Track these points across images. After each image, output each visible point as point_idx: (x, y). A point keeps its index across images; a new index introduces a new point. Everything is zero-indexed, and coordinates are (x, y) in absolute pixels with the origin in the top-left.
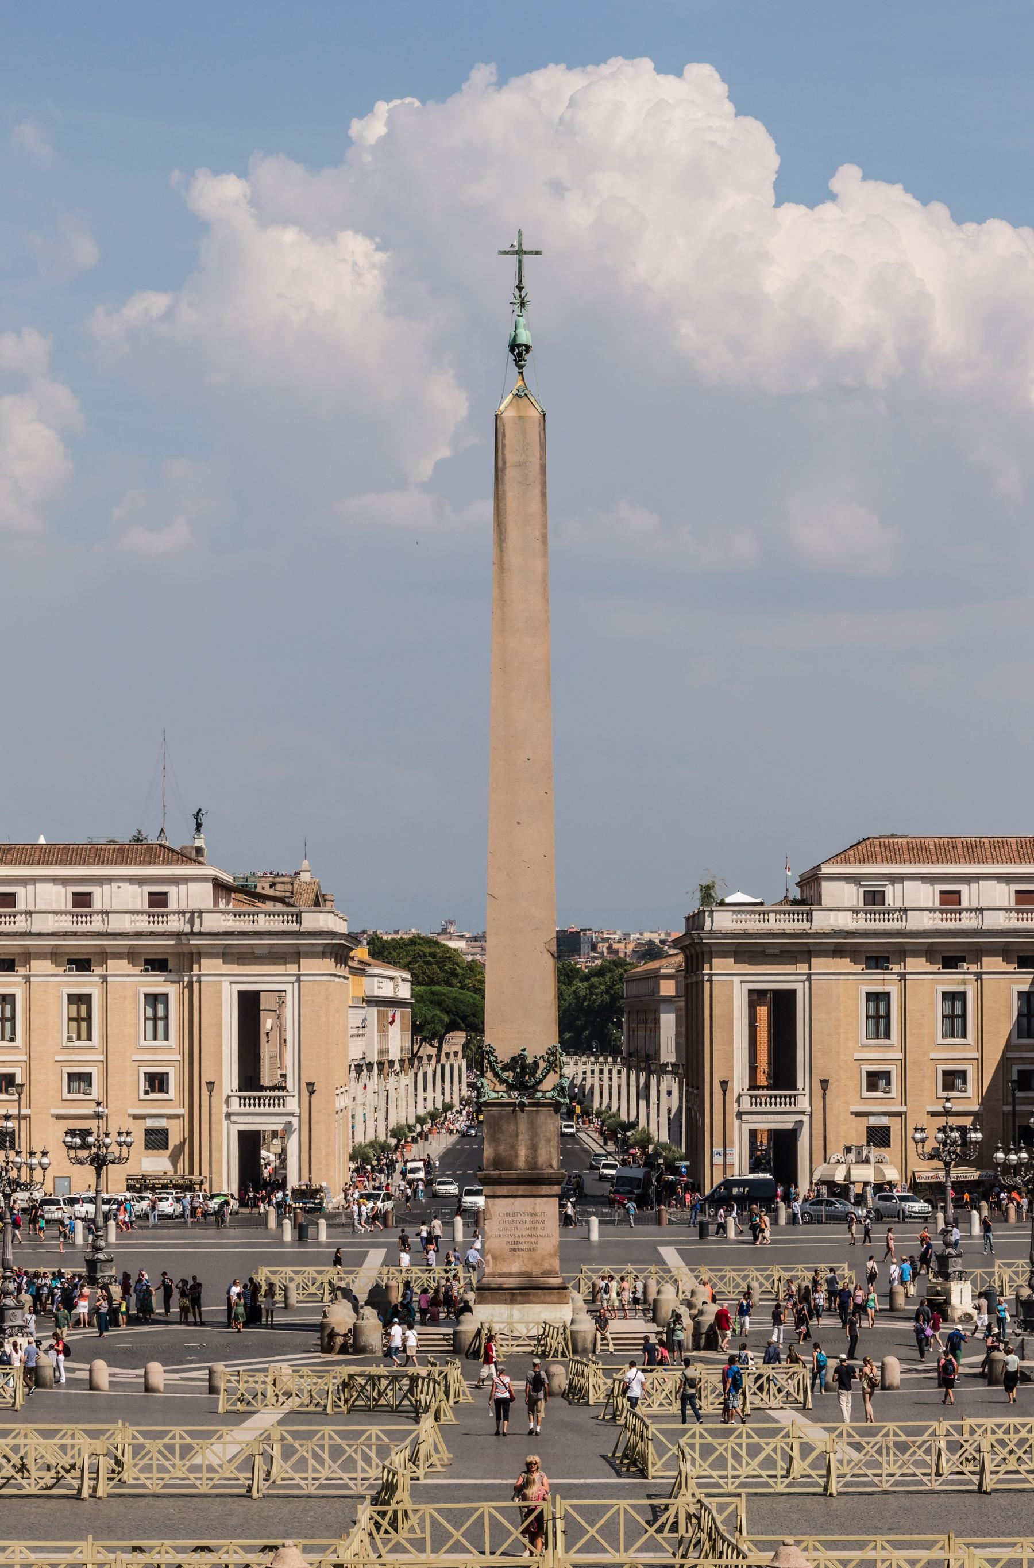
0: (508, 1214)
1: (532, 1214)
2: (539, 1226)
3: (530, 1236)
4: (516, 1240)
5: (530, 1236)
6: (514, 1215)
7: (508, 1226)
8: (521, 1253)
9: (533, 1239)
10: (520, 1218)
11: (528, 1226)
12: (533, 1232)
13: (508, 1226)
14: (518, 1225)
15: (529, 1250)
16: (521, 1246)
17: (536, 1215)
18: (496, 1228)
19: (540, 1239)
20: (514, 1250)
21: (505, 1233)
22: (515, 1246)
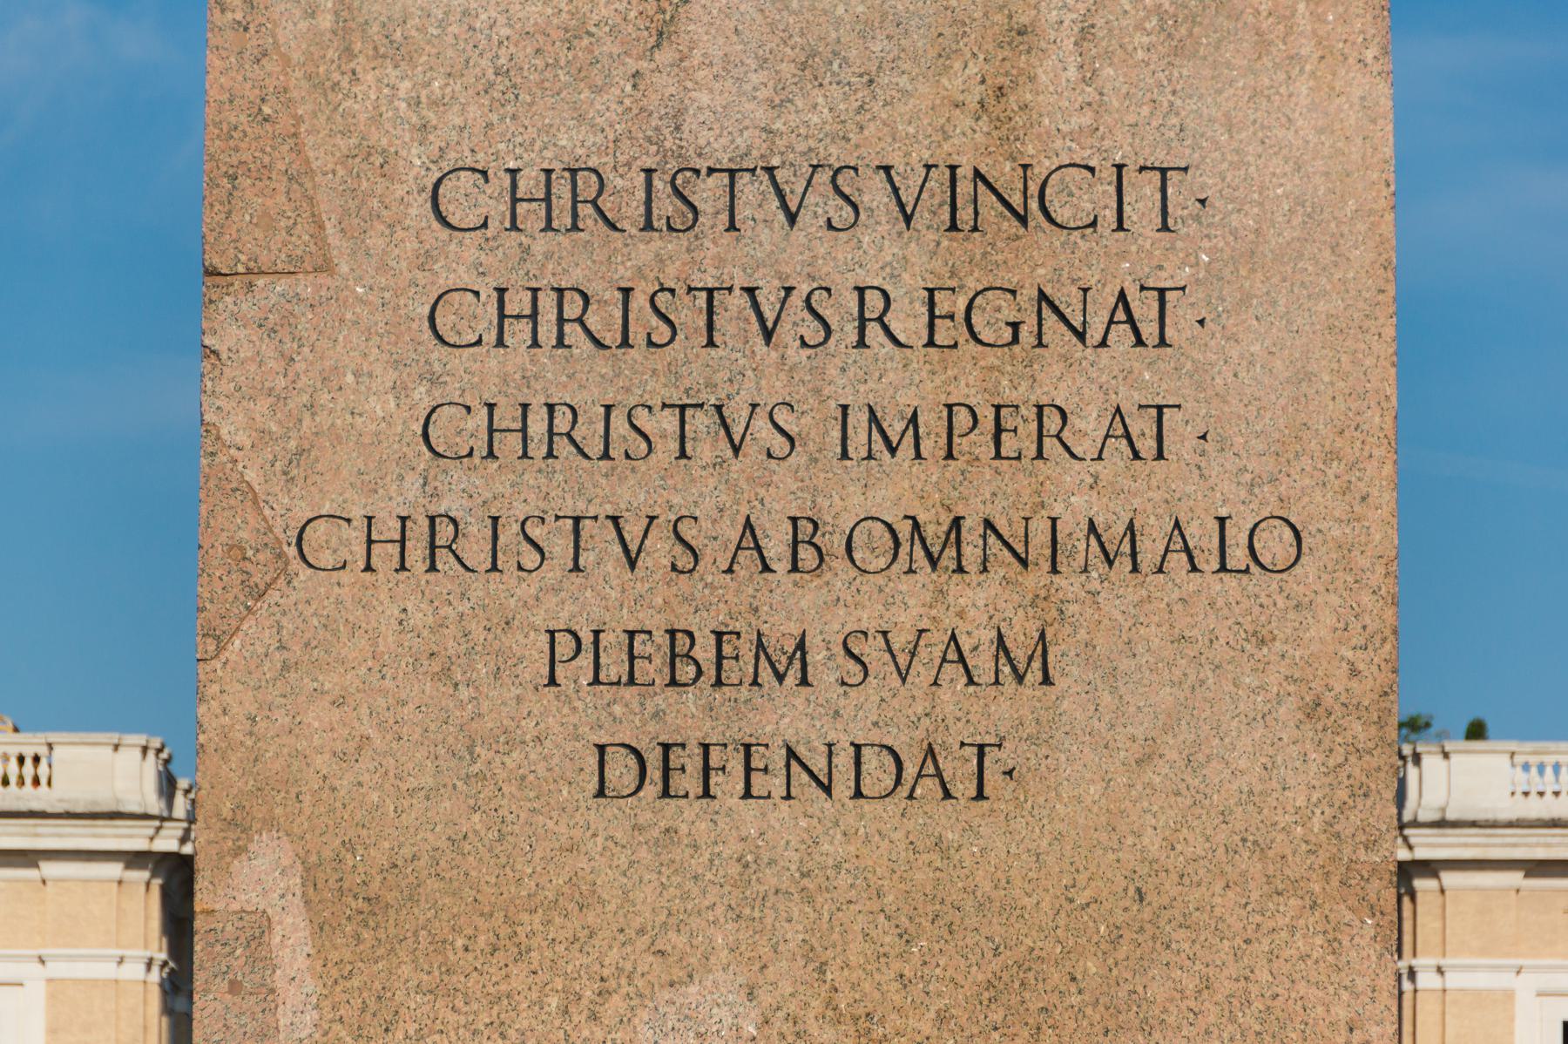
0: (572, 197)
1: (966, 200)
2: (1086, 383)
3: (936, 546)
4: (709, 603)
5: (936, 546)
6: (677, 196)
7: (584, 380)
8: (783, 824)
9: (982, 603)
10: (766, 251)
11: (903, 382)
12: (990, 492)
13: (584, 380)
14: (748, 372)
15: (920, 771)
16: (784, 716)
17: (1029, 209)
18: (386, 410)
19: (1101, 606)
20: (660, 768)
21: (519, 489)
22: (689, 715)
